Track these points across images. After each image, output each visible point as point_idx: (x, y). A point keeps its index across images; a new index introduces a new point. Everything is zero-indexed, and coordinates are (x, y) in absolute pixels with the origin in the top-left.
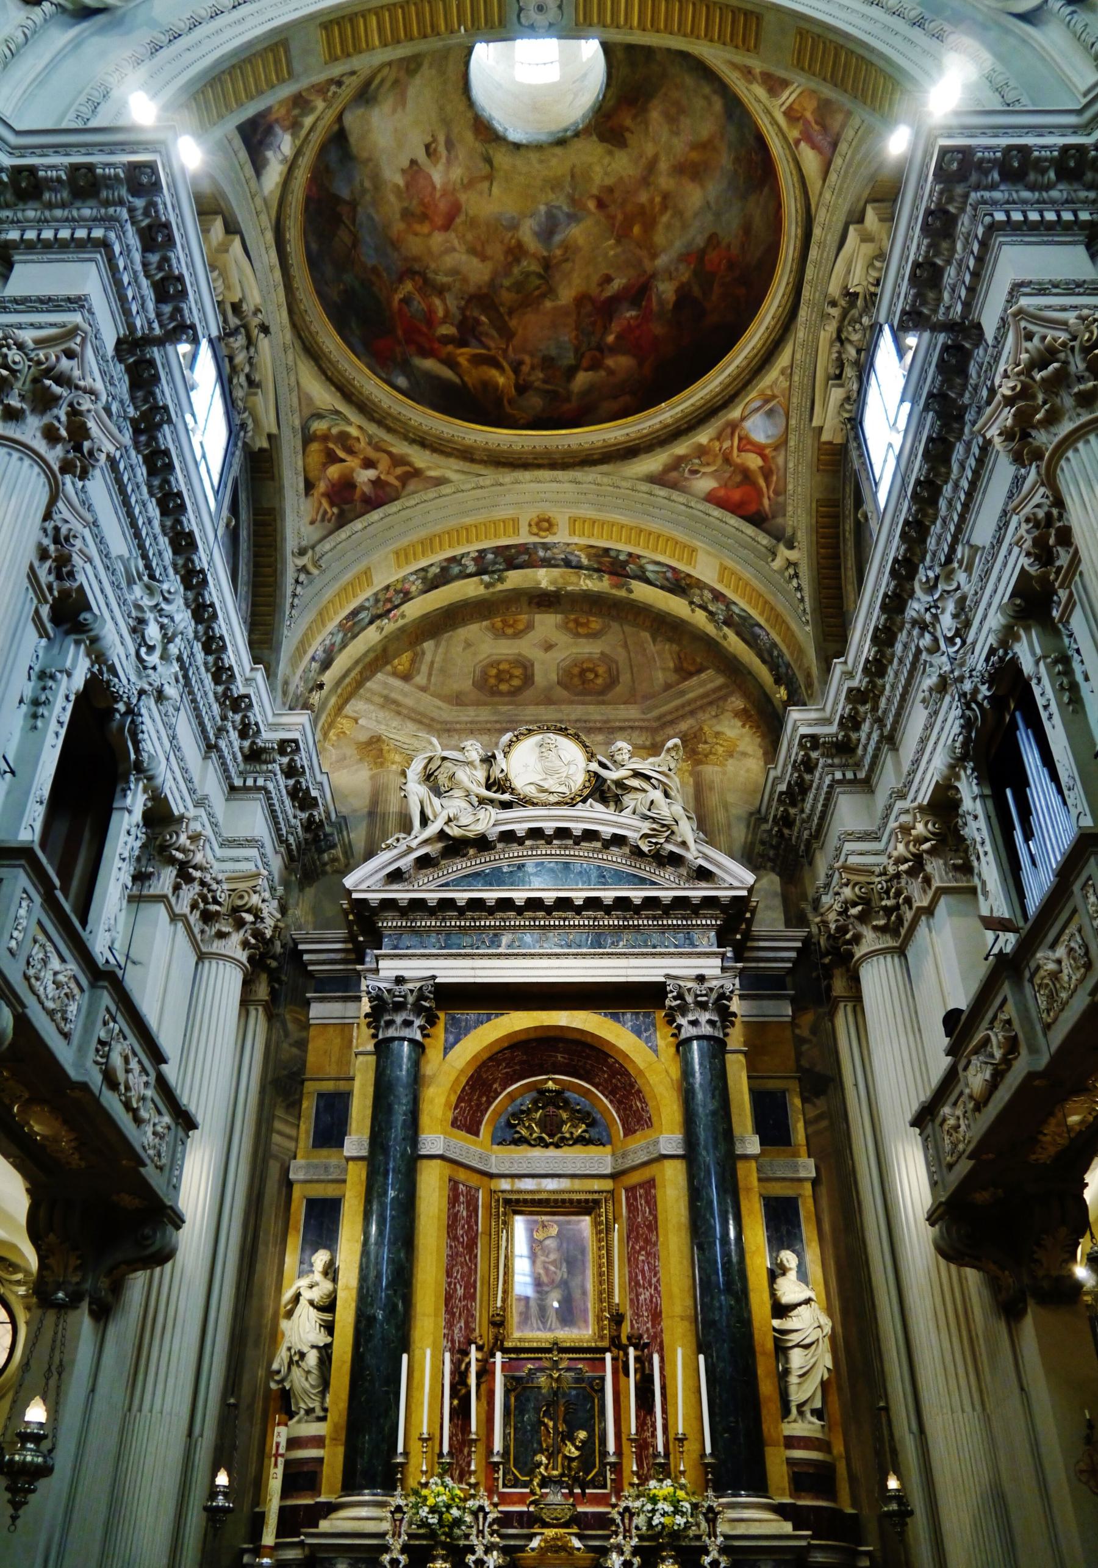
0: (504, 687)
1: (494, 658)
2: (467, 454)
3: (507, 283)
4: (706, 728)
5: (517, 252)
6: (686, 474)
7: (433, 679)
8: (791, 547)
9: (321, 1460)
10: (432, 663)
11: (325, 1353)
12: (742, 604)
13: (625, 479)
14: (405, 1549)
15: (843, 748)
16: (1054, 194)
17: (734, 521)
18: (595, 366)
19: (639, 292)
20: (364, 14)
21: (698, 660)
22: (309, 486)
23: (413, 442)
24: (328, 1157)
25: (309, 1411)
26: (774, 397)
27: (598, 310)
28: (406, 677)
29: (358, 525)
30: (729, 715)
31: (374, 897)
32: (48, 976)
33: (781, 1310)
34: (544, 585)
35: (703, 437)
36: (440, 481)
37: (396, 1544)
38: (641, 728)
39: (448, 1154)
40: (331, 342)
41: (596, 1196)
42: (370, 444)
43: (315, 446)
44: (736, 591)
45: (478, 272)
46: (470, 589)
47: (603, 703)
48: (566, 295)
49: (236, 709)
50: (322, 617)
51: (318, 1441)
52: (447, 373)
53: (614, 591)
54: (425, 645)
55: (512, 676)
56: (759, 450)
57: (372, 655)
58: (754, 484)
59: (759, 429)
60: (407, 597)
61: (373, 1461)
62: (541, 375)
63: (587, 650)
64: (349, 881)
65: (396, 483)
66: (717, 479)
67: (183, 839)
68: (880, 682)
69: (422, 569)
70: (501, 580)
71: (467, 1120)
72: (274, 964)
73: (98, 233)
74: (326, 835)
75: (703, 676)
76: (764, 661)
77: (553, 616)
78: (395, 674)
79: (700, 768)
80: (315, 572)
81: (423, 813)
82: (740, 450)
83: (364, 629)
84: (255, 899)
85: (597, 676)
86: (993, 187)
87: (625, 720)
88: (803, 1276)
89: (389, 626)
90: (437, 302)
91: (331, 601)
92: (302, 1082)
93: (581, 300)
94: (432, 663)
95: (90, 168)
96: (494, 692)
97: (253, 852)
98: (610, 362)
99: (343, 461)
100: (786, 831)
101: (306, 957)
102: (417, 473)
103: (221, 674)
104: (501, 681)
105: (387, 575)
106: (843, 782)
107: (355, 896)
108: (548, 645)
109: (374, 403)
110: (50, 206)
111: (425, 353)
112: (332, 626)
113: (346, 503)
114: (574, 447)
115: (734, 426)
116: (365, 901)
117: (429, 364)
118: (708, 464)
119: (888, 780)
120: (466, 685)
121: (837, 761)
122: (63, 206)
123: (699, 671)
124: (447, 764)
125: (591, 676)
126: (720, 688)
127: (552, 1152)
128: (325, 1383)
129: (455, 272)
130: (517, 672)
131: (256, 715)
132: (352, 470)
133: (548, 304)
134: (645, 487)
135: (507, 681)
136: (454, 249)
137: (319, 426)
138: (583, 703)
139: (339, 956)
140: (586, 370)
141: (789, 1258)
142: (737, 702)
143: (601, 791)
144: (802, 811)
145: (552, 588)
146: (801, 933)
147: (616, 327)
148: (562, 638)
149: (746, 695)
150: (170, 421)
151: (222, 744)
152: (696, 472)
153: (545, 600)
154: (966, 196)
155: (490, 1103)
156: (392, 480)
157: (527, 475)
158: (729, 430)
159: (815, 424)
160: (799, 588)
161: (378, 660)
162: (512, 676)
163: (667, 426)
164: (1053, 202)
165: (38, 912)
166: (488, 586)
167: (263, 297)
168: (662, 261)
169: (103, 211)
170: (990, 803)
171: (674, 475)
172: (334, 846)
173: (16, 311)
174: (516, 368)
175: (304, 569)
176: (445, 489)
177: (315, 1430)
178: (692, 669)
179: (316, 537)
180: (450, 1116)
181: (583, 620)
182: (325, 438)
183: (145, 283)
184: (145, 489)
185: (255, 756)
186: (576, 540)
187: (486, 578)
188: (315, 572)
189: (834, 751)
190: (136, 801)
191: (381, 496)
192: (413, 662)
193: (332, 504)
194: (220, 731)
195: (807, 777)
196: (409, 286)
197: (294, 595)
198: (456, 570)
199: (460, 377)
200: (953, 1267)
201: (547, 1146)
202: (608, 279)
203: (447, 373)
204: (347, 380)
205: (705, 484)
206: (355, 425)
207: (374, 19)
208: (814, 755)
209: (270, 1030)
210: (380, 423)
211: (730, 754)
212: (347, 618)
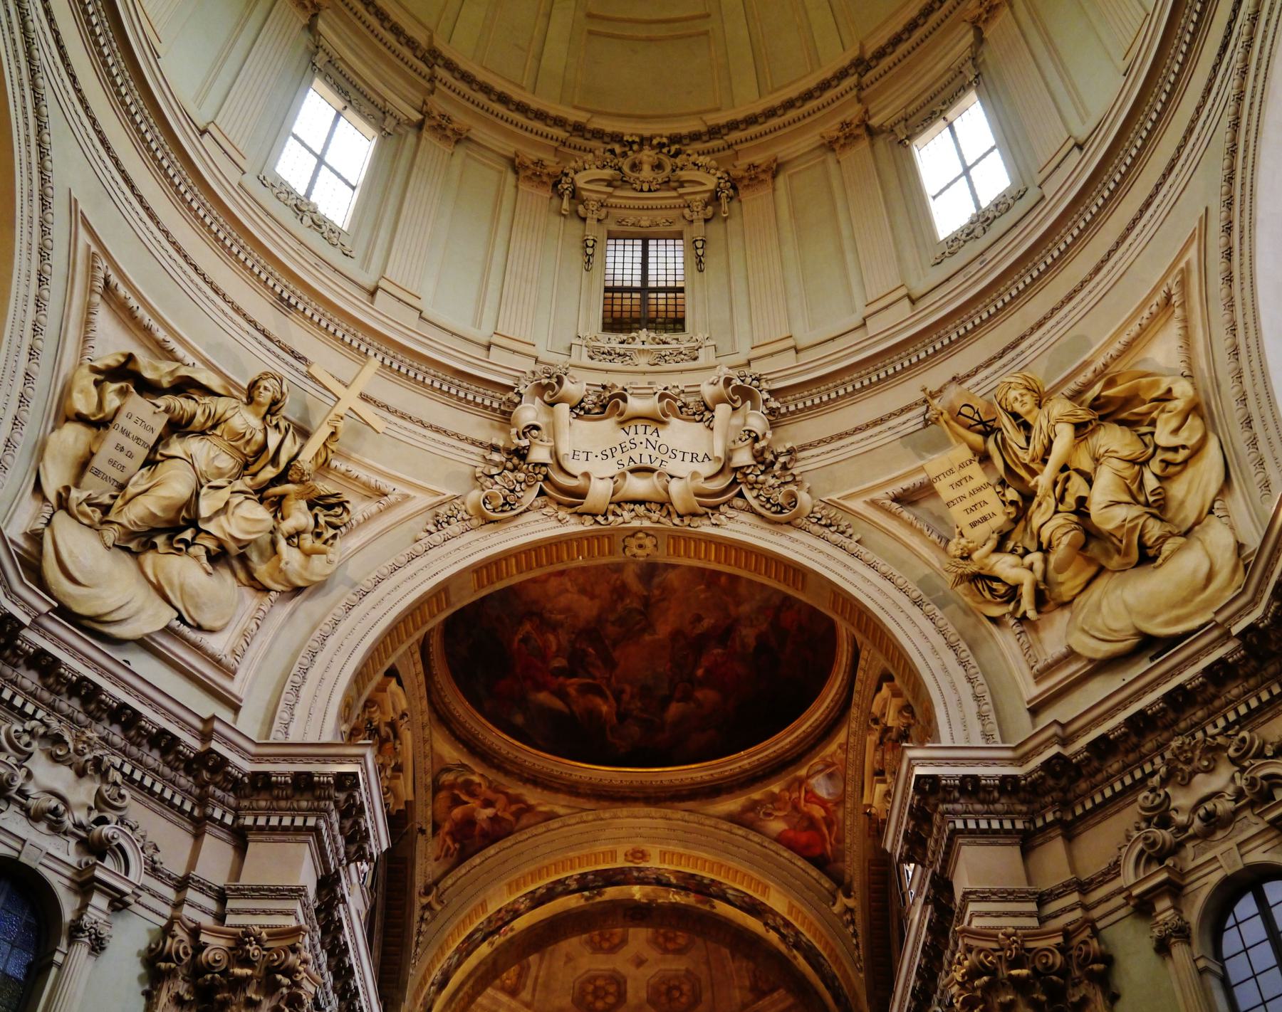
1: (592, 973)
2: (572, 789)
3: (612, 618)
5: (621, 591)
6: (761, 815)
7: (537, 994)
8: (848, 896)
10: (537, 978)
12: (808, 936)
13: (709, 816)
16: (998, 807)
17: (800, 863)
19: (724, 634)
20: (506, 559)
22: (436, 827)
26: (833, 764)
27: (690, 645)
28: (513, 992)
29: (477, 860)
34: (637, 897)
36: (551, 816)
40: (461, 708)
42: (489, 787)
43: (442, 794)
44: (803, 924)
45: (587, 608)
46: (573, 902)
48: (663, 630)
50: (442, 950)
52: (558, 704)
53: (699, 905)
54: (531, 958)
55: (607, 994)
56: (822, 803)
57: (483, 968)
58: (819, 830)
59: (822, 787)
60: (516, 914)
62: (639, 704)
63: (674, 967)
65: (511, 818)
66: (787, 822)
69: (532, 892)
70: (600, 894)
73: (311, 822)
75: (776, 995)
76: (828, 987)
77: (644, 930)
78: (503, 989)
80: (438, 908)
82: (806, 801)
83: (477, 946)
86: (955, 801)
89: (498, 940)
90: (551, 638)
91: (451, 935)
93: (676, 634)
94: (537, 978)
95: (309, 775)
98: (699, 695)
102: (529, 809)
104: (597, 997)
105: (498, 900)
109: (495, 752)
110: (278, 798)
111: (539, 687)
112: (449, 953)
113: (469, 840)
114: (666, 783)
115: (801, 782)
117: (543, 697)
118: (780, 809)
122: (287, 798)
123: (772, 990)
125: (677, 994)
129: (567, 610)
130: (612, 989)
132: (473, 810)
133: (647, 638)
134: (726, 825)
136: (567, 591)
137: (448, 778)
140: (678, 701)
145: (645, 901)
148: (651, 954)
150: (344, 902)
152: (770, 815)
153: (638, 913)
154: (937, 806)
156: (507, 816)
157: (624, 811)
158: (797, 785)
159: (865, 801)
160: (855, 935)
161: (486, 976)
162: (607, 994)
163: (746, 771)
164: (997, 813)
166: (587, 899)
167: (409, 703)
168: (745, 609)
171: (751, 815)
173: (253, 898)
174: (618, 696)
175: (427, 907)
176: (554, 824)
179: (439, 872)
181: (671, 935)
182: (452, 786)
183: (339, 838)
184: (319, 946)
186: (666, 866)
187: (586, 893)
188: (438, 908)
191: (497, 832)
192: (519, 976)
193: (454, 841)
196: (527, 627)
197: (419, 933)
198: (560, 888)
199: (568, 705)
202: (699, 619)
203: (558, 704)
204: (473, 735)
205: (777, 826)
206: (478, 774)
207: (514, 560)
212: (463, 943)
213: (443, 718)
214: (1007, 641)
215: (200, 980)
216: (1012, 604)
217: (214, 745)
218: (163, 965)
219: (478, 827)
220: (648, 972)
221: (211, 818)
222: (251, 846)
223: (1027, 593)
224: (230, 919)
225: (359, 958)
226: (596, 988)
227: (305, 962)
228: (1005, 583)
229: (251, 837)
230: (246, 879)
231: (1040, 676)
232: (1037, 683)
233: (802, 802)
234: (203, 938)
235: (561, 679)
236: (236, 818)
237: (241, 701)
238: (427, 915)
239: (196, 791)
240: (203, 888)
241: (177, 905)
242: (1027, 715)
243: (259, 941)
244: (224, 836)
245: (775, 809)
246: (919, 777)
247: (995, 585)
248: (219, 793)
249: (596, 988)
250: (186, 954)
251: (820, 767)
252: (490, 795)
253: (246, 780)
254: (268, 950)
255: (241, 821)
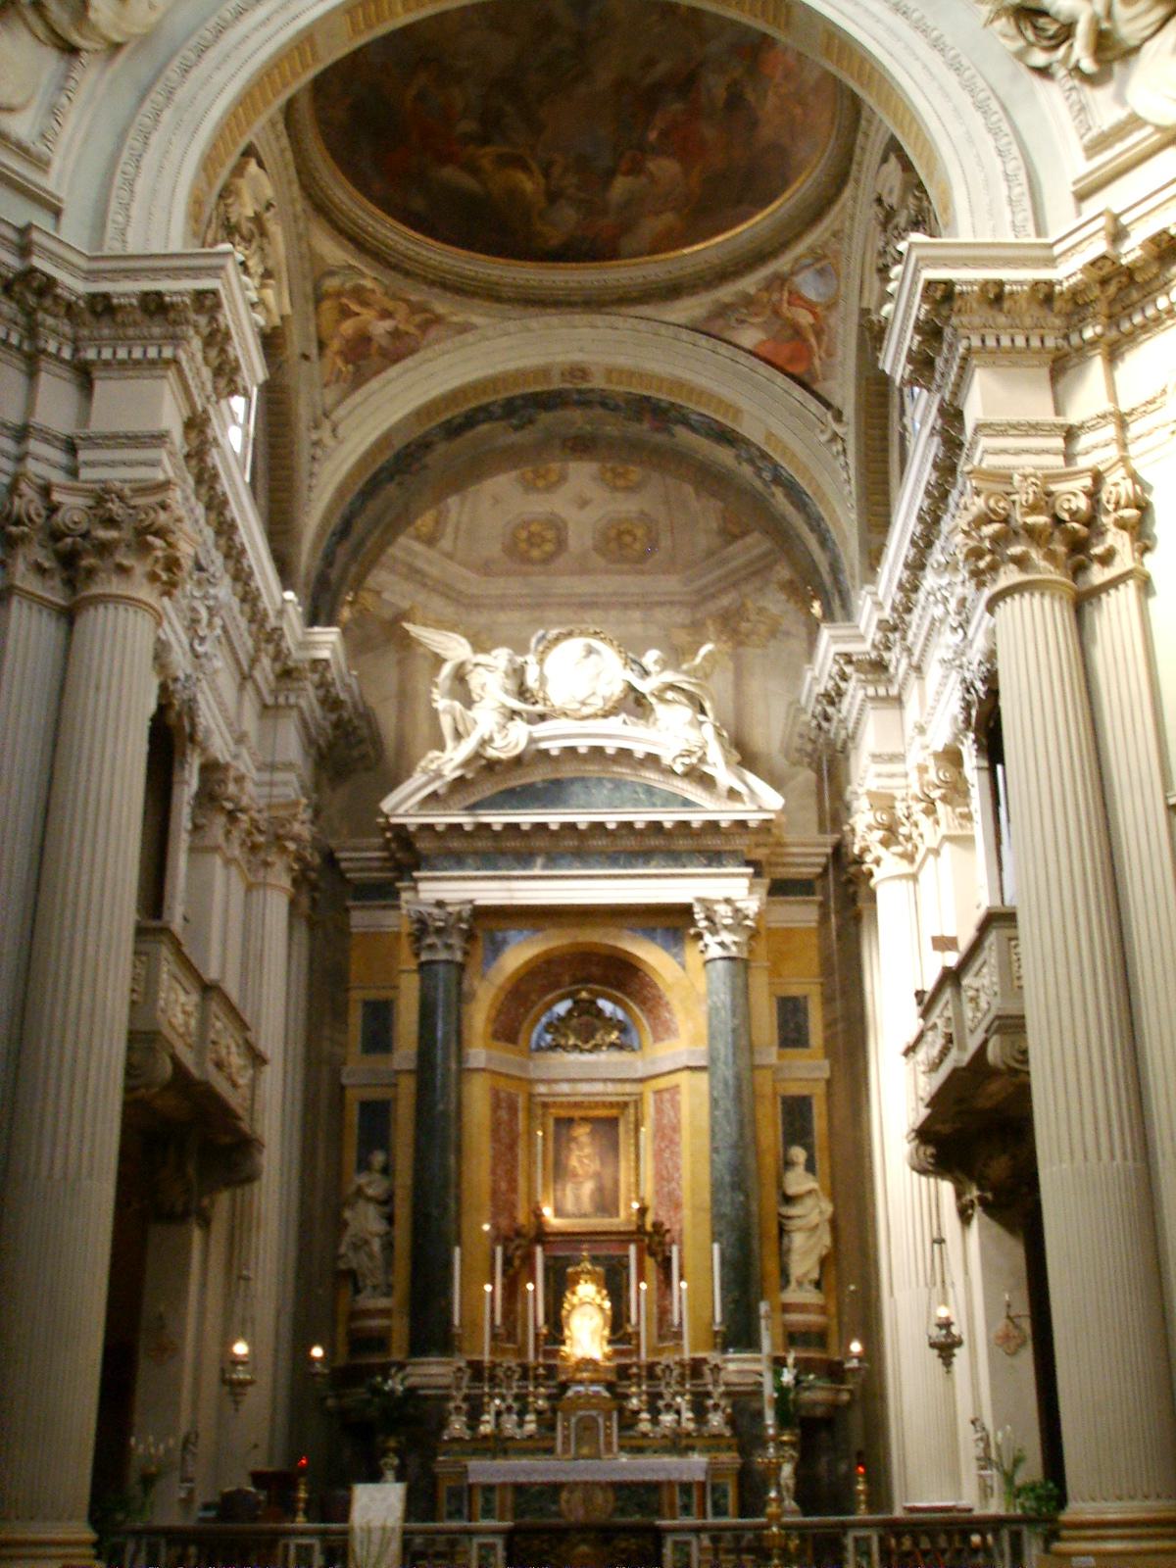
0: (535, 553)
4: (749, 604)
9: (389, 1329)
11: (389, 1246)
14: (466, 1398)
15: (879, 666)
18: (636, 169)
21: (744, 520)
22: (322, 346)
23: (432, 284)
24: (376, 1061)
25: (375, 1287)
28: (431, 541)
30: (773, 587)
31: (412, 822)
32: (178, 1009)
33: (788, 1200)
35: (749, 283)
37: (458, 1395)
38: (681, 603)
39: (492, 1067)
40: (342, 194)
41: (626, 1098)
42: (386, 294)
43: (327, 305)
47: (642, 573)
48: (604, 78)
49: (268, 641)
51: (386, 1313)
55: (544, 540)
56: (810, 307)
58: (805, 340)
61: (432, 1331)
64: (386, 805)
67: (232, 788)
68: (907, 617)
71: (507, 1031)
72: (313, 875)
73: (167, 353)
74: (355, 728)
75: (749, 540)
78: (418, 538)
79: (741, 650)
81: (456, 730)
82: (790, 303)
84: (297, 827)
85: (635, 539)
87: (665, 594)
88: (810, 1167)
92: (347, 990)
95: (159, 294)
96: (526, 559)
97: (292, 777)
98: (651, 166)
99: (358, 314)
100: (825, 725)
101: (344, 865)
102: (438, 320)
103: (257, 617)
106: (876, 698)
107: (394, 820)
108: (582, 498)
110: (124, 325)
116: (403, 826)
117: (449, 173)
118: (756, 315)
119: (912, 711)
120: (494, 549)
121: (870, 677)
122: (135, 324)
123: (744, 534)
124: (480, 669)
125: (627, 539)
126: (765, 555)
127: (587, 1057)
128: (389, 1264)
130: (550, 534)
131: (289, 642)
135: (539, 546)
137: (332, 284)
138: (621, 573)
139: (376, 864)
140: (627, 173)
141: (799, 1154)
142: (783, 572)
143: (635, 704)
144: (839, 711)
146: (831, 838)
147: (660, 122)
148: (596, 492)
149: (794, 564)
150: (218, 445)
151: (257, 674)
152: (742, 322)
155: (527, 1011)
156: (412, 329)
158: (779, 282)
162: (544, 540)
165: (175, 969)
169: (171, 329)
170: (985, 775)
172: (361, 741)
173: (108, 447)
176: (469, 337)
177: (384, 1306)
178: (737, 530)
180: (490, 1029)
181: (621, 470)
182: (339, 294)
185: (287, 674)
189: (867, 667)
190: (194, 762)
192: (437, 522)
193: (347, 362)
194: (254, 661)
195: (843, 685)
200: (924, 1179)
201: (582, 1051)
202: (650, 62)
203: (469, 183)
206: (370, 278)
208: (848, 669)
209: (312, 938)
210: (394, 267)
211: (773, 633)
213: (321, 208)
214: (1053, 96)
215: (60, 545)
216: (1063, 50)
217: (37, 262)
218: (13, 529)
219: (375, 345)
220: (593, 515)
221: (44, 351)
222: (99, 387)
223: (1082, 30)
224: (85, 474)
225: (242, 510)
226: (531, 535)
227: (179, 520)
228: (1056, 20)
229: (96, 374)
230: (99, 425)
231: (1094, 148)
232: (1089, 158)
233: (785, 305)
234: (56, 497)
235: (471, 149)
236: (76, 350)
237: (59, 200)
238: (319, 452)
239: (21, 319)
240: (47, 437)
241: (20, 459)
242: (1070, 200)
243: (121, 498)
244: (67, 375)
245: (750, 315)
246: (930, 284)
247: (1042, 21)
248: (50, 321)
249: (531, 535)
250: (39, 515)
251: (808, 261)
252: (390, 305)
253: (81, 303)
254: (134, 507)
255: (82, 354)
